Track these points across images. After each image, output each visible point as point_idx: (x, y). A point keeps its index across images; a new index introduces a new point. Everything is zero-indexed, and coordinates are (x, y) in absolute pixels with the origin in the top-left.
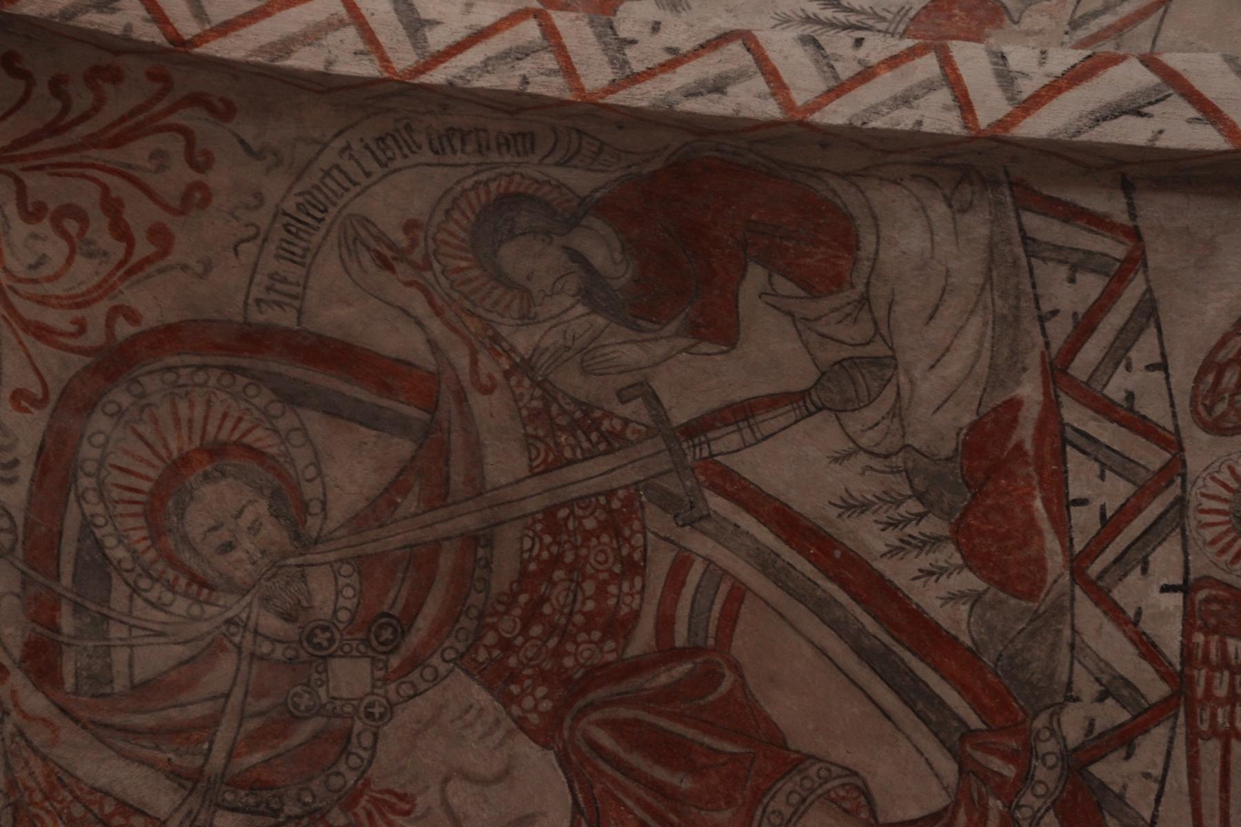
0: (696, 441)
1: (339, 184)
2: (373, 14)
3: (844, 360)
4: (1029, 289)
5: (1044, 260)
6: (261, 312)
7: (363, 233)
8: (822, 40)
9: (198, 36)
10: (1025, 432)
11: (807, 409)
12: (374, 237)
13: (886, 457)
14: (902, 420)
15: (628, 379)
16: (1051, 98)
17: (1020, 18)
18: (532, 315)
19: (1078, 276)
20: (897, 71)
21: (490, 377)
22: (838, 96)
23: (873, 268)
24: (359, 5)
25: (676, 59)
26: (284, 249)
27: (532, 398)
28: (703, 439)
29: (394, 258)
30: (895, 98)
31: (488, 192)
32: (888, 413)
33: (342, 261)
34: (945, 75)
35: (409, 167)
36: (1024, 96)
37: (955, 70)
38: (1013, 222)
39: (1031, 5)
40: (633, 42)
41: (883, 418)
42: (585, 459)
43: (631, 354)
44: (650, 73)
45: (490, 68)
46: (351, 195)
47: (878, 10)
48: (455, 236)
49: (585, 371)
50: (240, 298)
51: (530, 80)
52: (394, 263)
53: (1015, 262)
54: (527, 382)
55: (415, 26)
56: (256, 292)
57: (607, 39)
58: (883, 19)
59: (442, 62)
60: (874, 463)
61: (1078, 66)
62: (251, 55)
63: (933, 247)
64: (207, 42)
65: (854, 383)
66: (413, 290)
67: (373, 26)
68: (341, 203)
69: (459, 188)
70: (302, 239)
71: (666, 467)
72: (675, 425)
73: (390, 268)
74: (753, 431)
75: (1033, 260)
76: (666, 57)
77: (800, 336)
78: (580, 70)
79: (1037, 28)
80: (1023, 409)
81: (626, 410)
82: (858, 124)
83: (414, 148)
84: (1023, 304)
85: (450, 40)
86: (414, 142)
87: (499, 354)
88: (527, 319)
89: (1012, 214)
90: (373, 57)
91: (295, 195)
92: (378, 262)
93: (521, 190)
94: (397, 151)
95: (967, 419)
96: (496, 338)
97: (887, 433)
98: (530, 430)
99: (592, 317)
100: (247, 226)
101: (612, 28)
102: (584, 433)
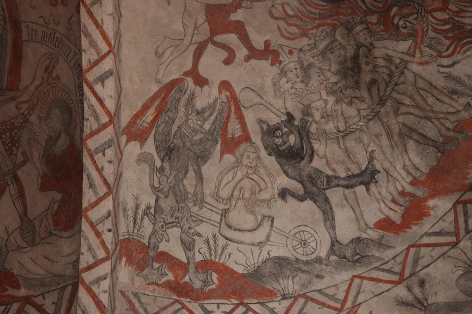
0: (13, 179)
1: (66, 52)
2: (103, 64)
3: (35, 228)
4: (52, 289)
5: (59, 293)
6: (25, 27)
7: (54, 61)
8: (110, 218)
9: (86, 4)
10: (11, 292)
11: (22, 217)
12: (53, 65)
13: (6, 246)
14: (16, 249)
15: (29, 155)
16: (91, 296)
17: (139, 276)
18: (42, 121)
19: (54, 305)
20: (99, 245)
21: (21, 108)
22: (91, 226)
23: (59, 236)
24: (106, 59)
25: (100, 170)
26: (45, 34)
27: (18, 123)
28: (14, 181)
29: (48, 73)
30: (90, 245)
31: (71, 104)
32: (19, 245)
33: (45, 54)
34: (99, 261)
35: (74, 76)
36: (92, 287)
37: (100, 264)
38: (69, 283)
39: (144, 278)
40: (104, 155)
41: (17, 243)
42: (2, 142)
43: (36, 155)
44: (94, 162)
45: (90, 107)
46: (64, 56)
47: (142, 228)
48: (58, 93)
49: (29, 139)
50: (27, 20)
51: (88, 122)
52: (47, 73)
53: (59, 284)
54: (22, 121)
55: (102, 79)
56: (30, 25)
57: (104, 146)
58: (139, 230)
59: (90, 90)
60: (4, 241)
61: (101, 303)
62: (83, 23)
63: (64, 256)
64: (84, 7)
65: (28, 232)
66: (41, 80)
67: (100, 65)
68: (61, 52)
69: (70, 94)
70: (49, 40)
71: (3, 170)
72: (17, 171)
73: (45, 72)
74: (16, 198)
75: (59, 290)
76: (100, 167)
77: (42, 213)
78: (93, 138)
79: (135, 282)
80: (17, 290)
81: (19, 155)
82: (82, 234)
83: (78, 78)
84: (47, 288)
85: (98, 92)
86: (80, 78)
87: (28, 110)
88: (40, 119)
89: (71, 282)
90: (89, 66)
91: (61, 36)
92: (47, 67)
93: (73, 115)
94: (77, 72)
95: (15, 272)
96: (33, 109)
97: (13, 245)
98: (8, 123)
99: (44, 141)
100: (49, 20)
101: (108, 147)
102: (11, 141)
